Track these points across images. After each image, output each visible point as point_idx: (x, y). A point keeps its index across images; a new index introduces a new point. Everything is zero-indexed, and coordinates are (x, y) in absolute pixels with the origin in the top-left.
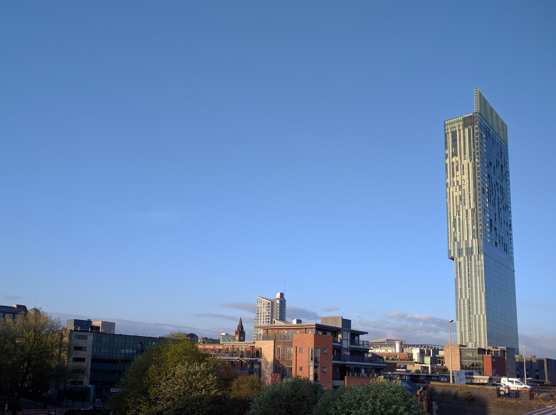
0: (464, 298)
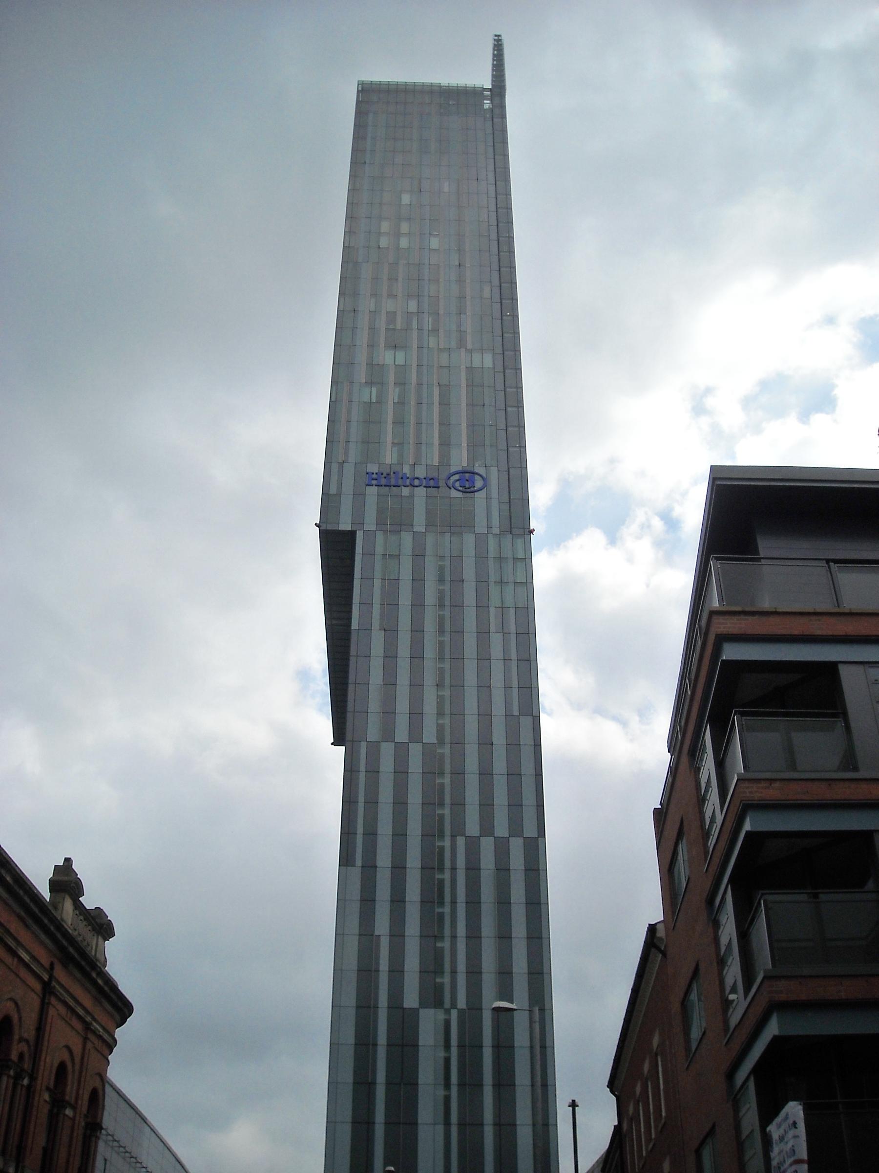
0: (402, 735)
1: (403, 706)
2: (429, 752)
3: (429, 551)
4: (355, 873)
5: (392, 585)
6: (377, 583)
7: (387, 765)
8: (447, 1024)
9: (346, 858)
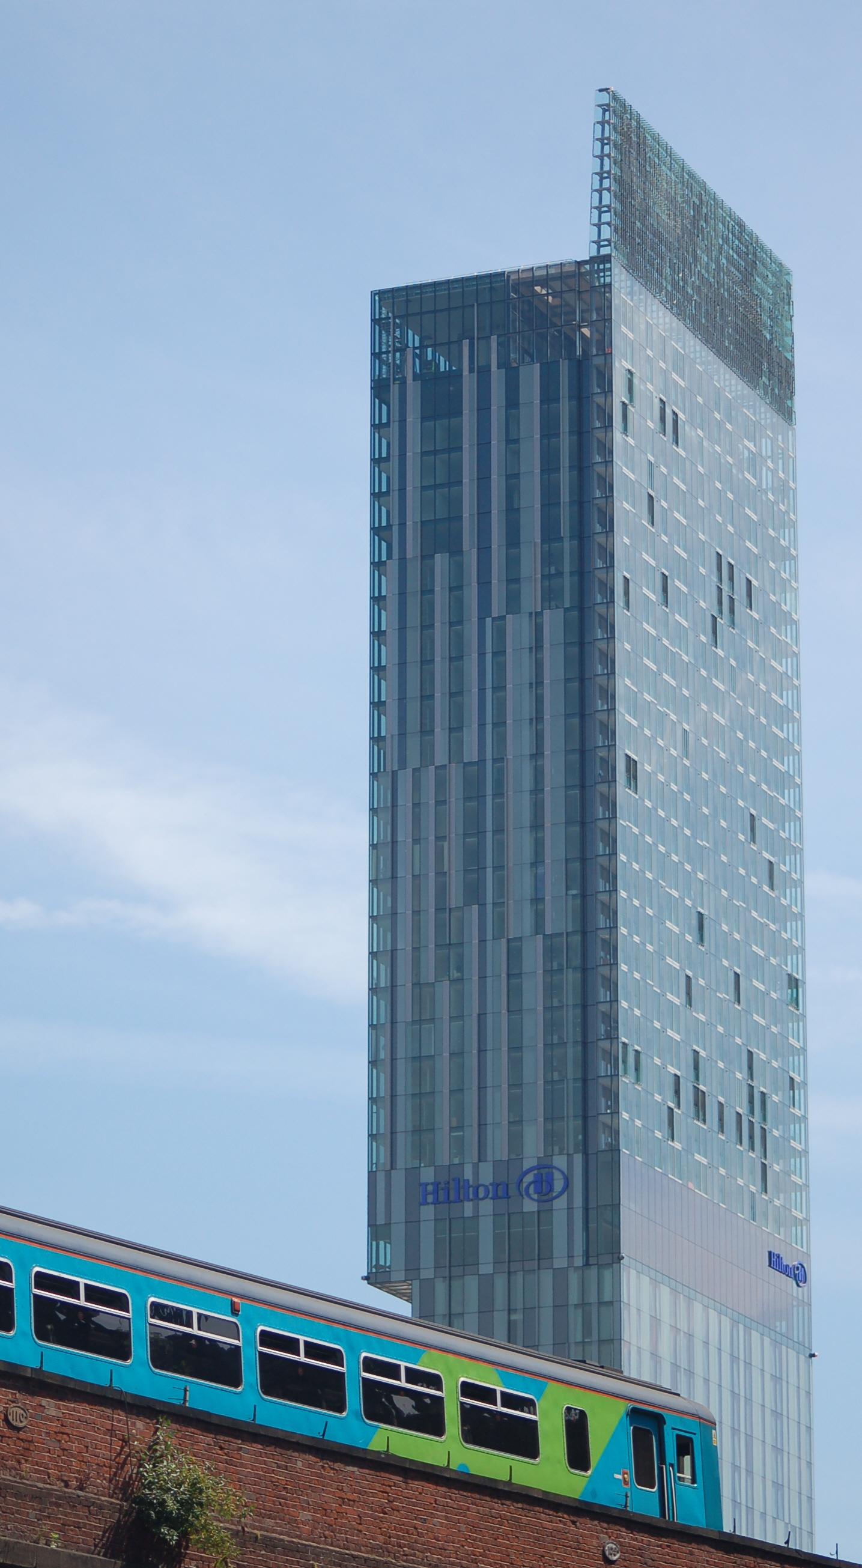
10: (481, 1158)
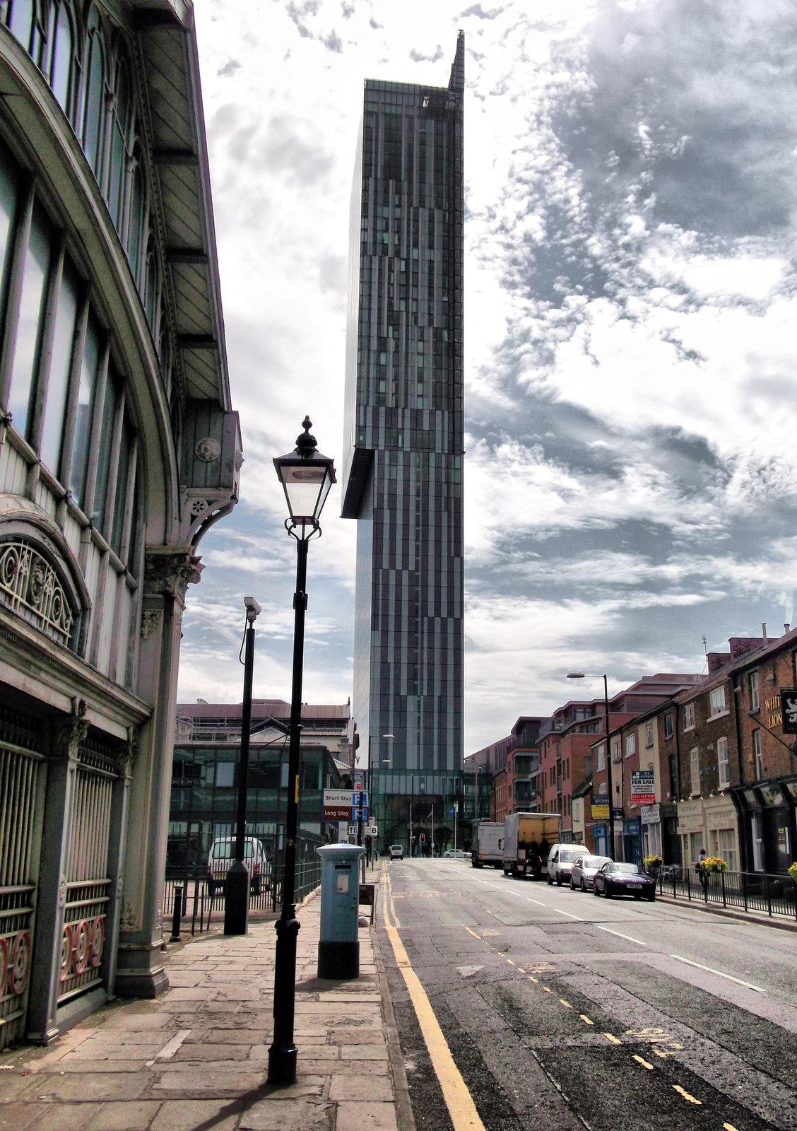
0: (399, 566)
1: (399, 550)
2: (411, 574)
3: (412, 463)
4: (379, 633)
5: (393, 482)
6: (386, 482)
7: (392, 581)
8: (419, 701)
9: (374, 628)
10: (406, 406)
